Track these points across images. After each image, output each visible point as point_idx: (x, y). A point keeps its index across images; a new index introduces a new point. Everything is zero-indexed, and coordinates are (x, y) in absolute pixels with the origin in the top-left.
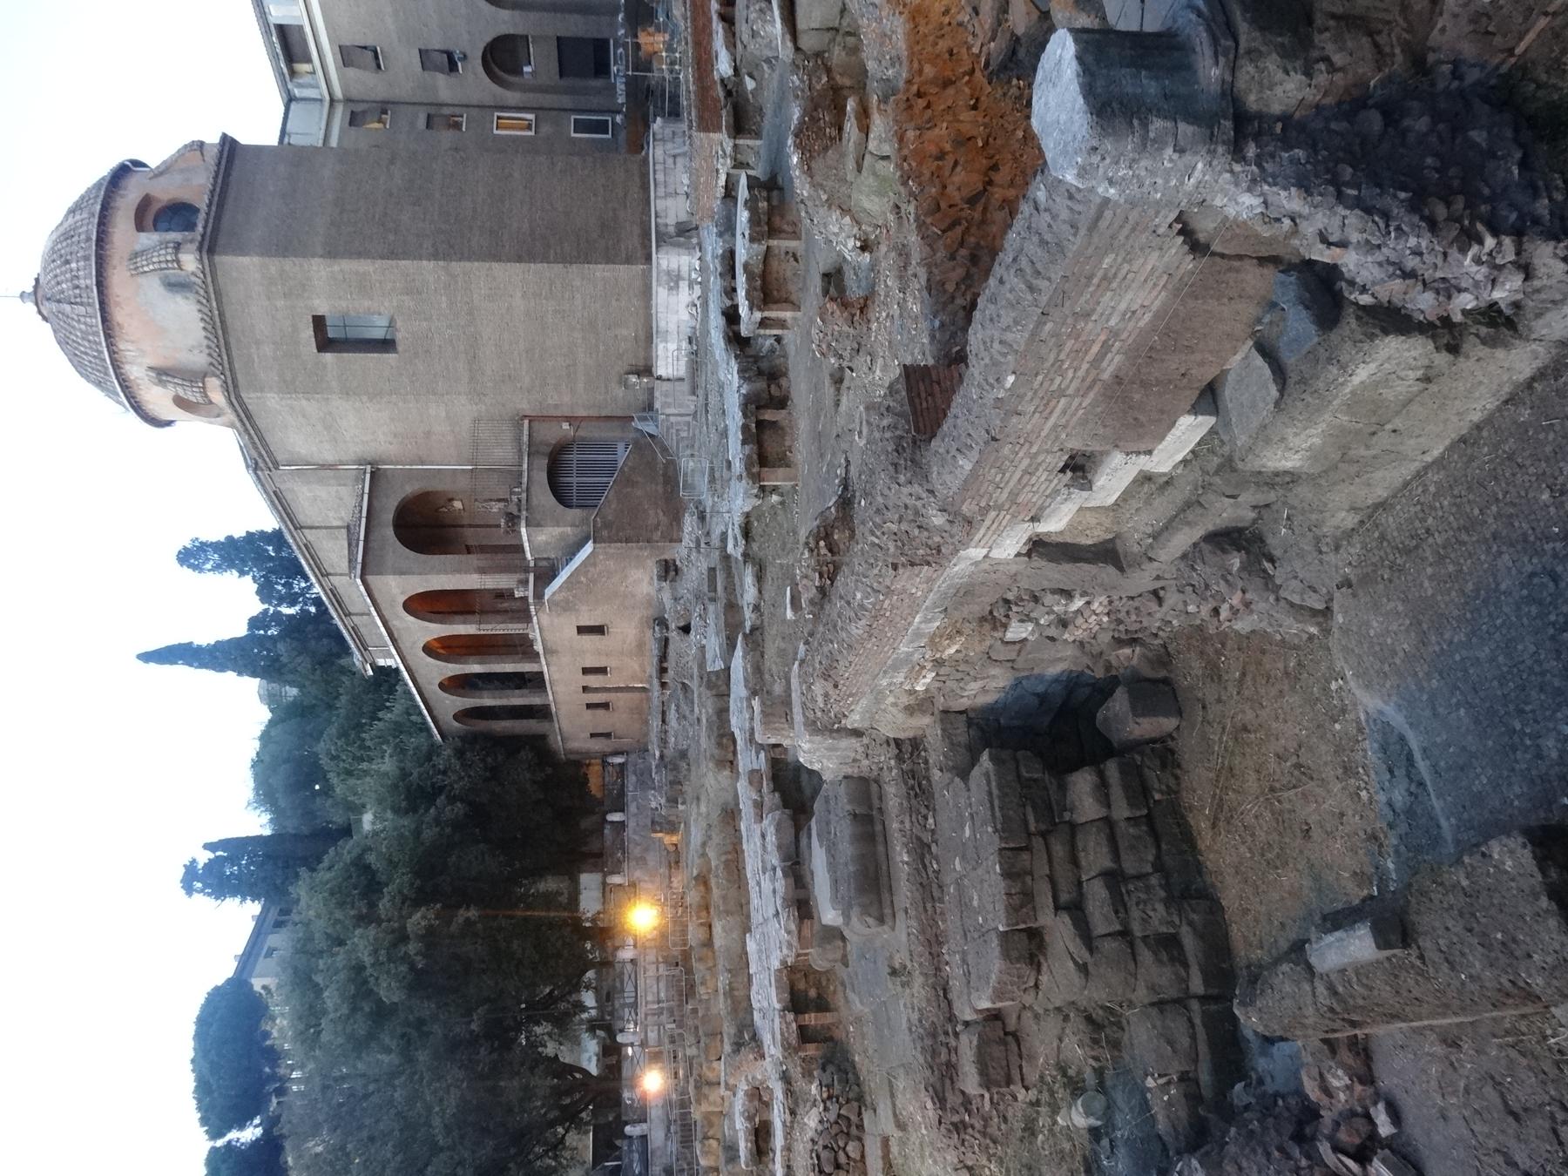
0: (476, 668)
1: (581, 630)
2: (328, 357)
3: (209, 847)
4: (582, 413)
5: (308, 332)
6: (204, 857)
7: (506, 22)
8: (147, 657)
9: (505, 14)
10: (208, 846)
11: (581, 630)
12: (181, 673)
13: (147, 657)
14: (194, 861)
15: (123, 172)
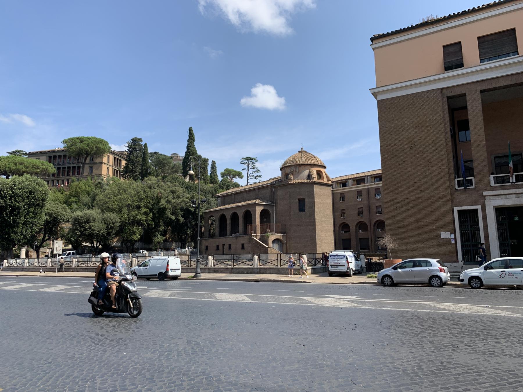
0: (228, 222)
1: (243, 245)
2: (297, 200)
3: (146, 144)
4: (288, 245)
5: (301, 197)
6: (143, 143)
7: (353, 228)
8: (190, 130)
9: (354, 228)
10: (146, 144)
11: (243, 245)
12: (187, 138)
13: (190, 130)
14: (142, 141)
15: (325, 167)
